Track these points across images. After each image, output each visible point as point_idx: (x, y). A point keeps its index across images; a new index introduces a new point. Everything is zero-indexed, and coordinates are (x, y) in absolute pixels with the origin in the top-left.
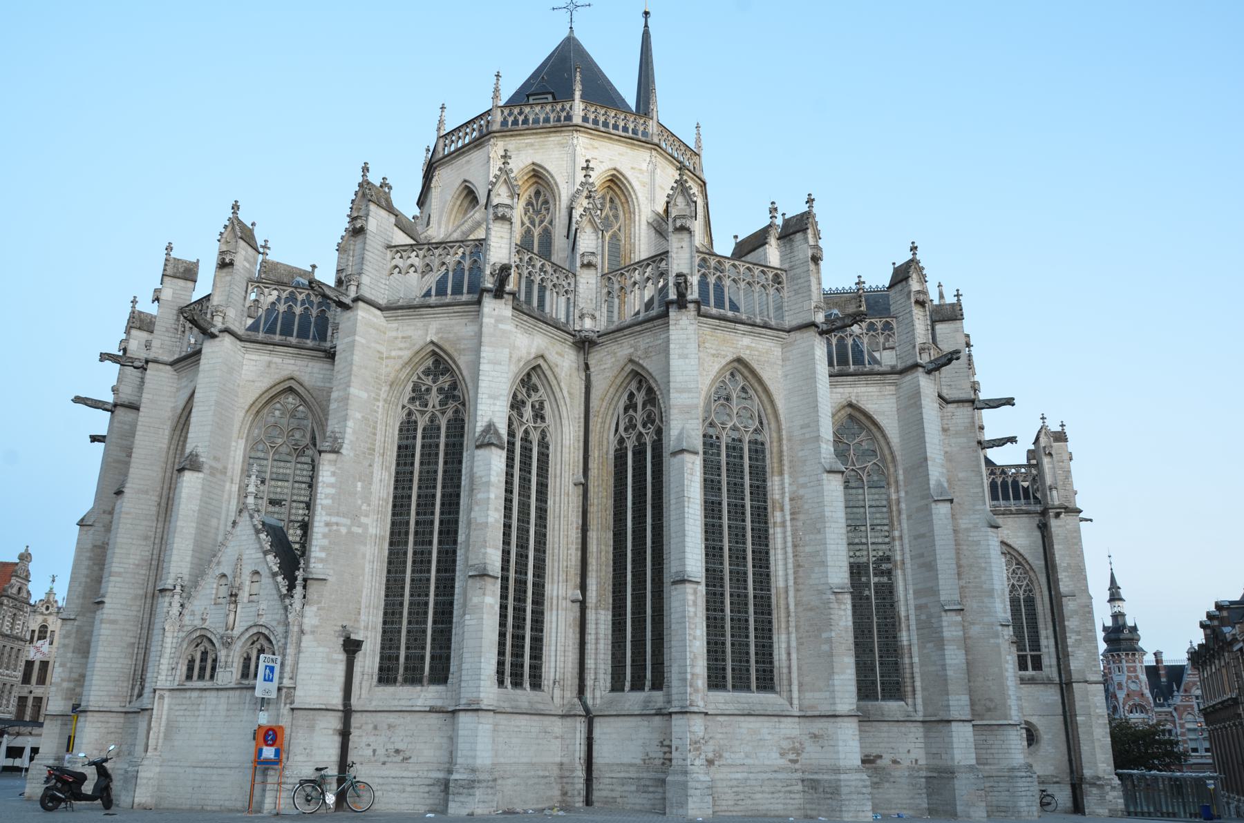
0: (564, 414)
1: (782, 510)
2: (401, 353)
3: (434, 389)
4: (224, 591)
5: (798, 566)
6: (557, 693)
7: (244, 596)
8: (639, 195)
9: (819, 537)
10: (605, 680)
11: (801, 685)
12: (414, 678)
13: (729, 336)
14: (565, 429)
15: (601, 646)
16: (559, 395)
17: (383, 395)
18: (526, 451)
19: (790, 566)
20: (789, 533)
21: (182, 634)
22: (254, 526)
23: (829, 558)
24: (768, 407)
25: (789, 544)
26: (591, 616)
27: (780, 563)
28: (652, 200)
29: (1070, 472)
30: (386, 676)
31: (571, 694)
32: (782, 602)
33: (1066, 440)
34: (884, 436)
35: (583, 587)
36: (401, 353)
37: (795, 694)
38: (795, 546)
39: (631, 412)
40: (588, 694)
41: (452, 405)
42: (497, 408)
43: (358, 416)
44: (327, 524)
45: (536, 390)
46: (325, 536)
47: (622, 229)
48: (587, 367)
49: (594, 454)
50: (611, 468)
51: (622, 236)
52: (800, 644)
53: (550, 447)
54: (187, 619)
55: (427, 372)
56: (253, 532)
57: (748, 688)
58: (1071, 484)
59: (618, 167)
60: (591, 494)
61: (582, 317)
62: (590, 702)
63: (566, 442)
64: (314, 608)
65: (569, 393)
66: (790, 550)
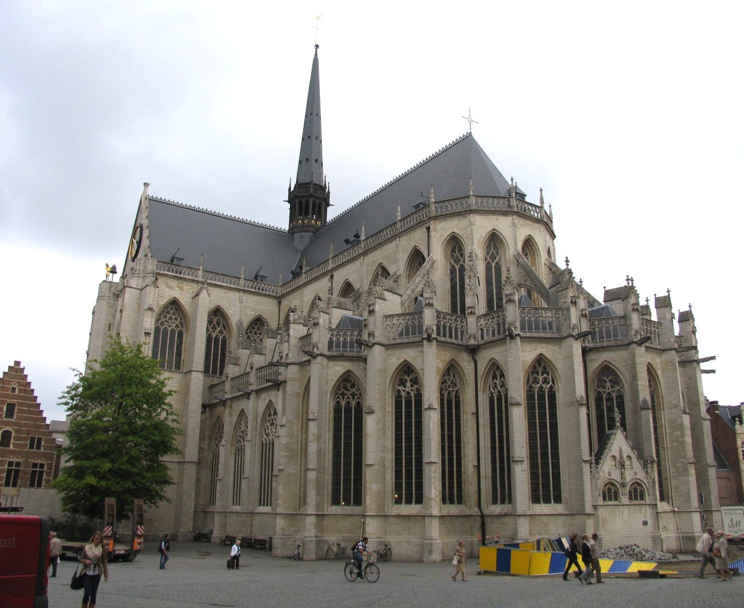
3: (408, 382)
18: (450, 401)
39: (495, 381)
41: (415, 387)
53: (461, 398)
57: (550, 502)
59: (496, 228)
61: (470, 338)
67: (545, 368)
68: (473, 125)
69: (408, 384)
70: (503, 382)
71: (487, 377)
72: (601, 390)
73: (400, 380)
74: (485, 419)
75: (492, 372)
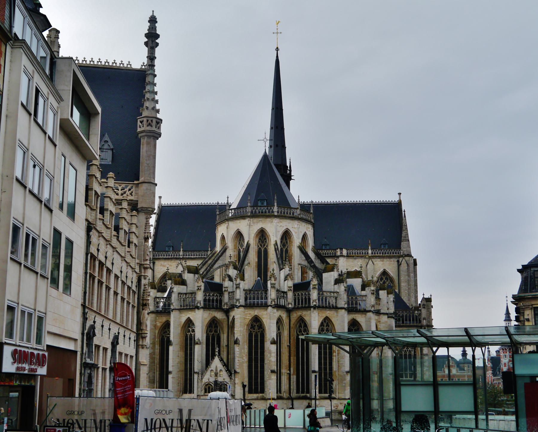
0: (284, 328)
1: (336, 352)
2: (249, 317)
3: (256, 327)
4: (213, 374)
5: (338, 366)
6: (285, 394)
7: (218, 375)
8: (294, 237)
9: (344, 360)
10: (295, 391)
11: (338, 393)
12: (256, 392)
13: (324, 311)
14: (285, 332)
15: (294, 384)
16: (283, 324)
17: (245, 328)
19: (337, 366)
20: (337, 358)
21: (203, 383)
22: (220, 359)
23: (346, 365)
24: (333, 328)
25: (337, 361)
26: (292, 377)
27: (335, 365)
28: (298, 238)
29: (431, 312)
30: (250, 392)
31: (288, 395)
32: (335, 374)
33: (431, 301)
34: (362, 328)
36: (249, 317)
37: (337, 394)
38: (338, 361)
40: (292, 395)
42: (274, 334)
43: (242, 334)
44: (238, 360)
46: (238, 363)
47: (289, 247)
48: (289, 317)
49: (292, 338)
50: (295, 341)
52: (338, 383)
54: (204, 380)
55: (254, 321)
56: (219, 361)
58: (431, 317)
60: (291, 348)
61: (289, 304)
62: (292, 396)
63: (285, 335)
64: (237, 379)
66: (337, 362)
67: (327, 323)
69: (256, 327)
70: (305, 329)
71: (296, 325)
73: (252, 325)
74: (293, 349)
75: (299, 324)
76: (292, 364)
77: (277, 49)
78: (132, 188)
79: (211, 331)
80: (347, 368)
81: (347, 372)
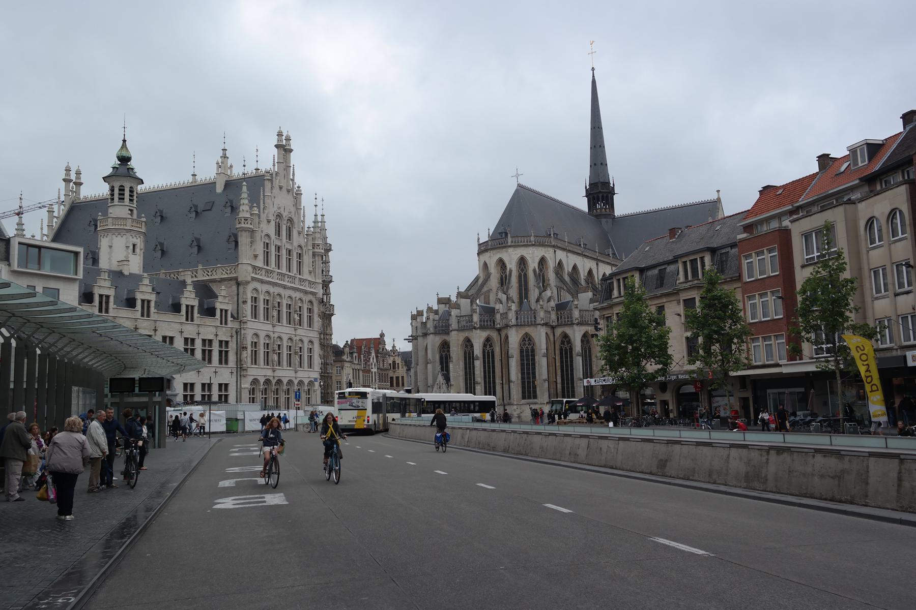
7: (441, 387)
26: (504, 386)
31: (501, 401)
35: (502, 381)
45: (490, 341)
48: (500, 335)
49: (503, 353)
51: (527, 273)
65: (497, 341)
67: (529, 338)
68: (520, 178)
72: (562, 346)
73: (466, 345)
76: (504, 375)
77: (593, 69)
78: (217, 269)
79: (444, 351)
80: (545, 376)
81: (545, 380)
